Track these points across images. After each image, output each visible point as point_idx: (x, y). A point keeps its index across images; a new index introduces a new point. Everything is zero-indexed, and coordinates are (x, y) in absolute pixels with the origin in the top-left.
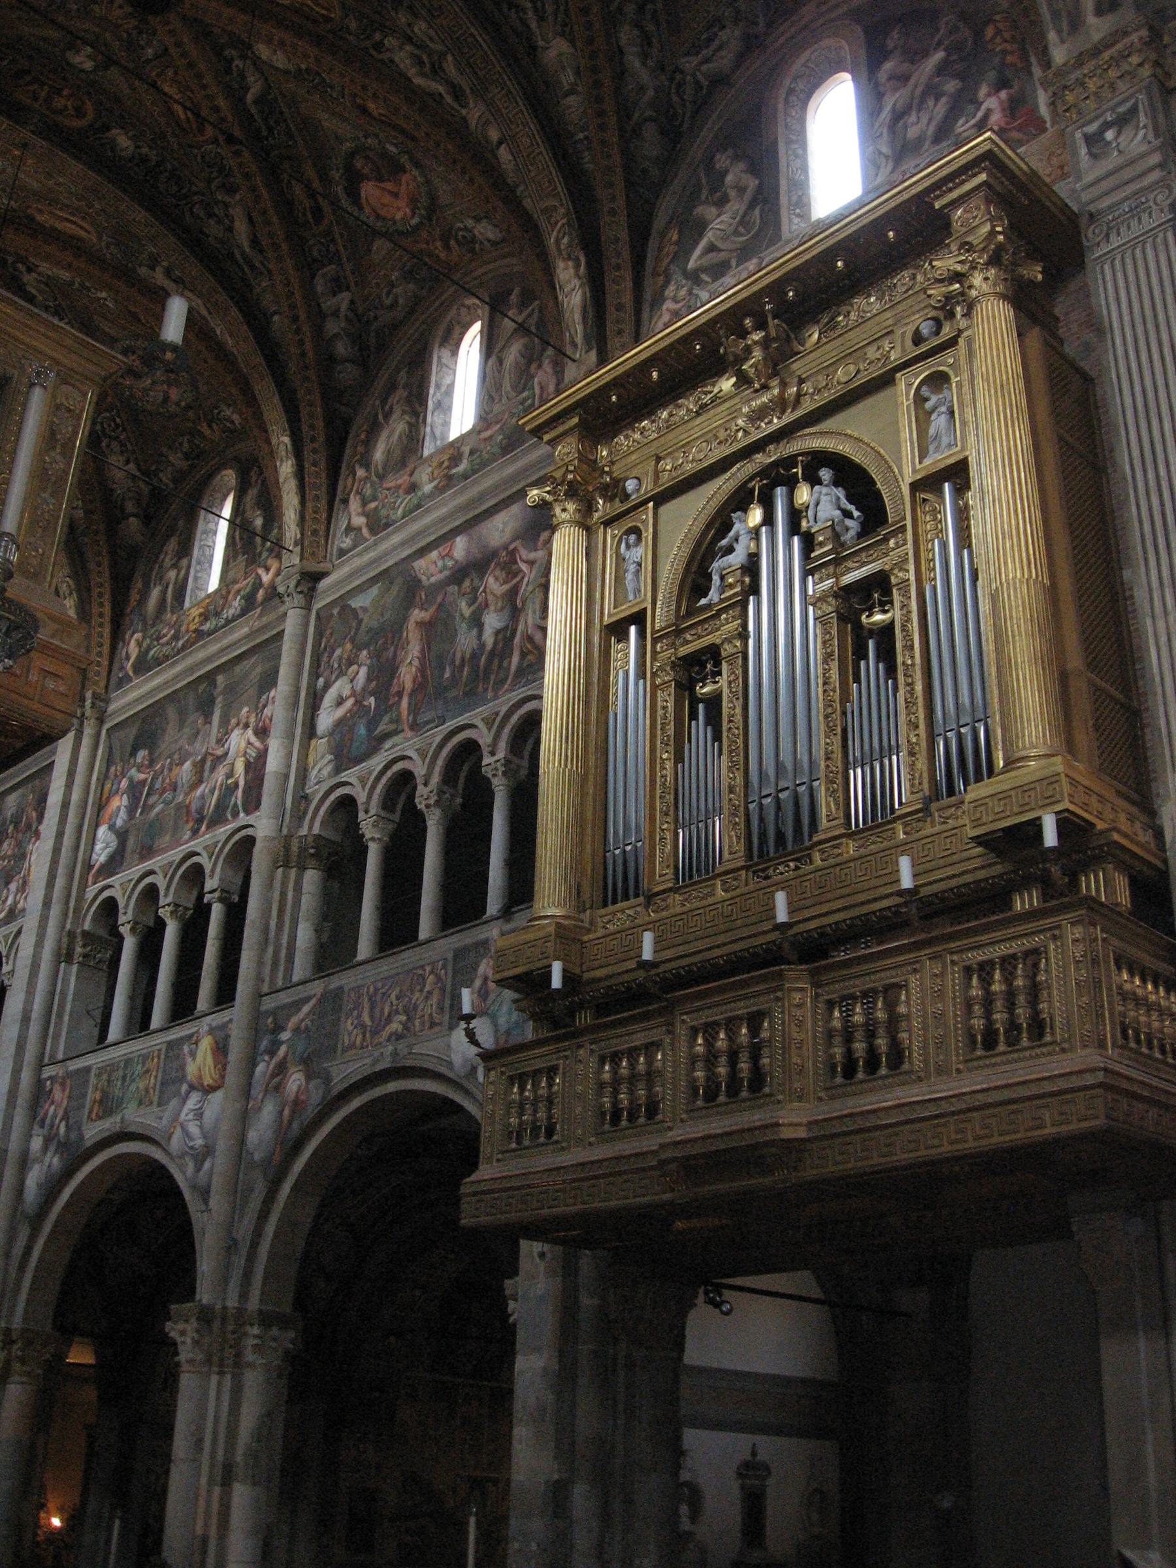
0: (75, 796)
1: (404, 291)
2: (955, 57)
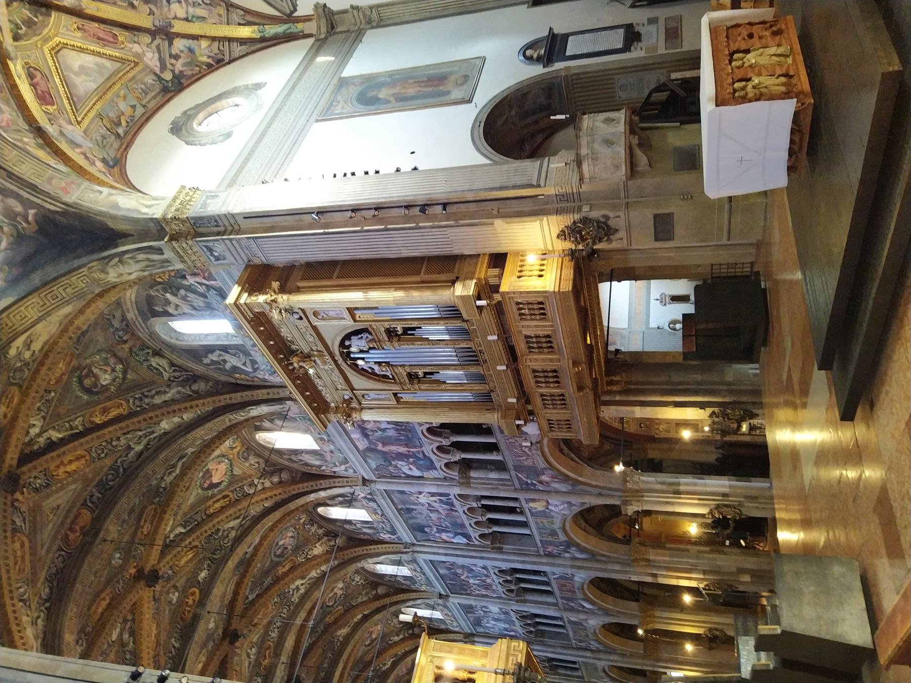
0: (442, 551)
1: (253, 460)
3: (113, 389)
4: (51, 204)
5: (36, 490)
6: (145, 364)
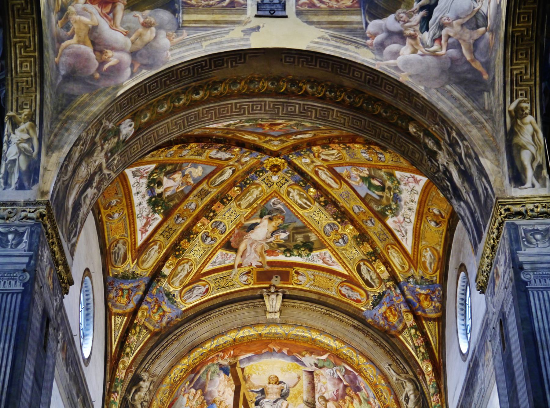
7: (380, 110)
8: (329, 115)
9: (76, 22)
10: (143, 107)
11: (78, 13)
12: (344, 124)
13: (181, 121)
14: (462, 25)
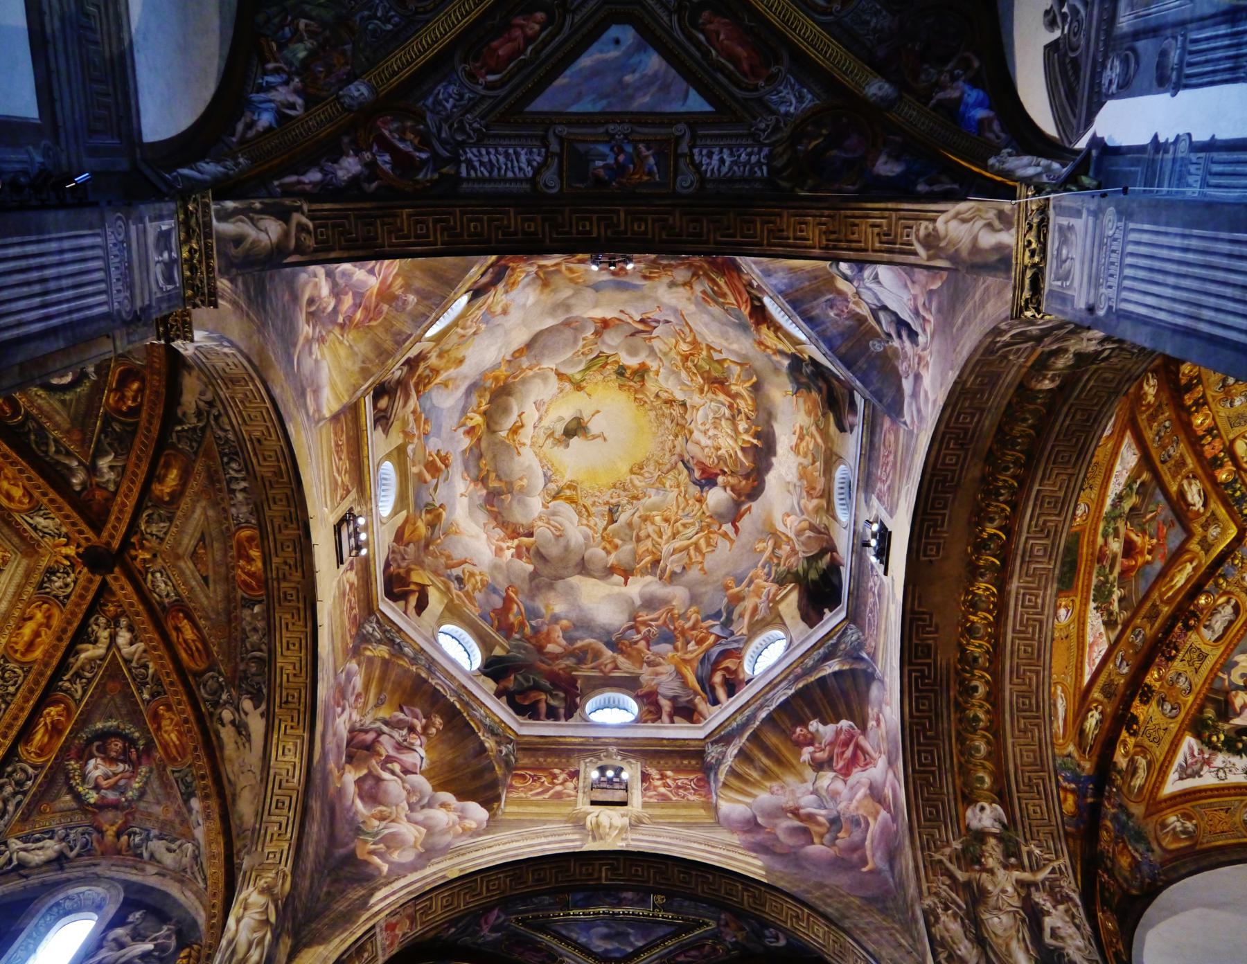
2: (156, 954)
3: (73, 764)
4: (386, 897)
5: (51, 571)
6: (61, 832)
7: (1020, 428)
8: (1051, 497)
9: (857, 808)
10: (957, 782)
11: (851, 800)
12: (1072, 475)
13: (1022, 721)
14: (913, 282)
